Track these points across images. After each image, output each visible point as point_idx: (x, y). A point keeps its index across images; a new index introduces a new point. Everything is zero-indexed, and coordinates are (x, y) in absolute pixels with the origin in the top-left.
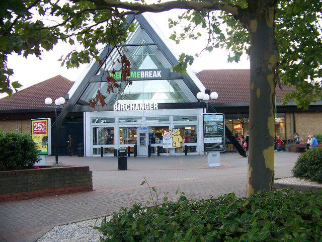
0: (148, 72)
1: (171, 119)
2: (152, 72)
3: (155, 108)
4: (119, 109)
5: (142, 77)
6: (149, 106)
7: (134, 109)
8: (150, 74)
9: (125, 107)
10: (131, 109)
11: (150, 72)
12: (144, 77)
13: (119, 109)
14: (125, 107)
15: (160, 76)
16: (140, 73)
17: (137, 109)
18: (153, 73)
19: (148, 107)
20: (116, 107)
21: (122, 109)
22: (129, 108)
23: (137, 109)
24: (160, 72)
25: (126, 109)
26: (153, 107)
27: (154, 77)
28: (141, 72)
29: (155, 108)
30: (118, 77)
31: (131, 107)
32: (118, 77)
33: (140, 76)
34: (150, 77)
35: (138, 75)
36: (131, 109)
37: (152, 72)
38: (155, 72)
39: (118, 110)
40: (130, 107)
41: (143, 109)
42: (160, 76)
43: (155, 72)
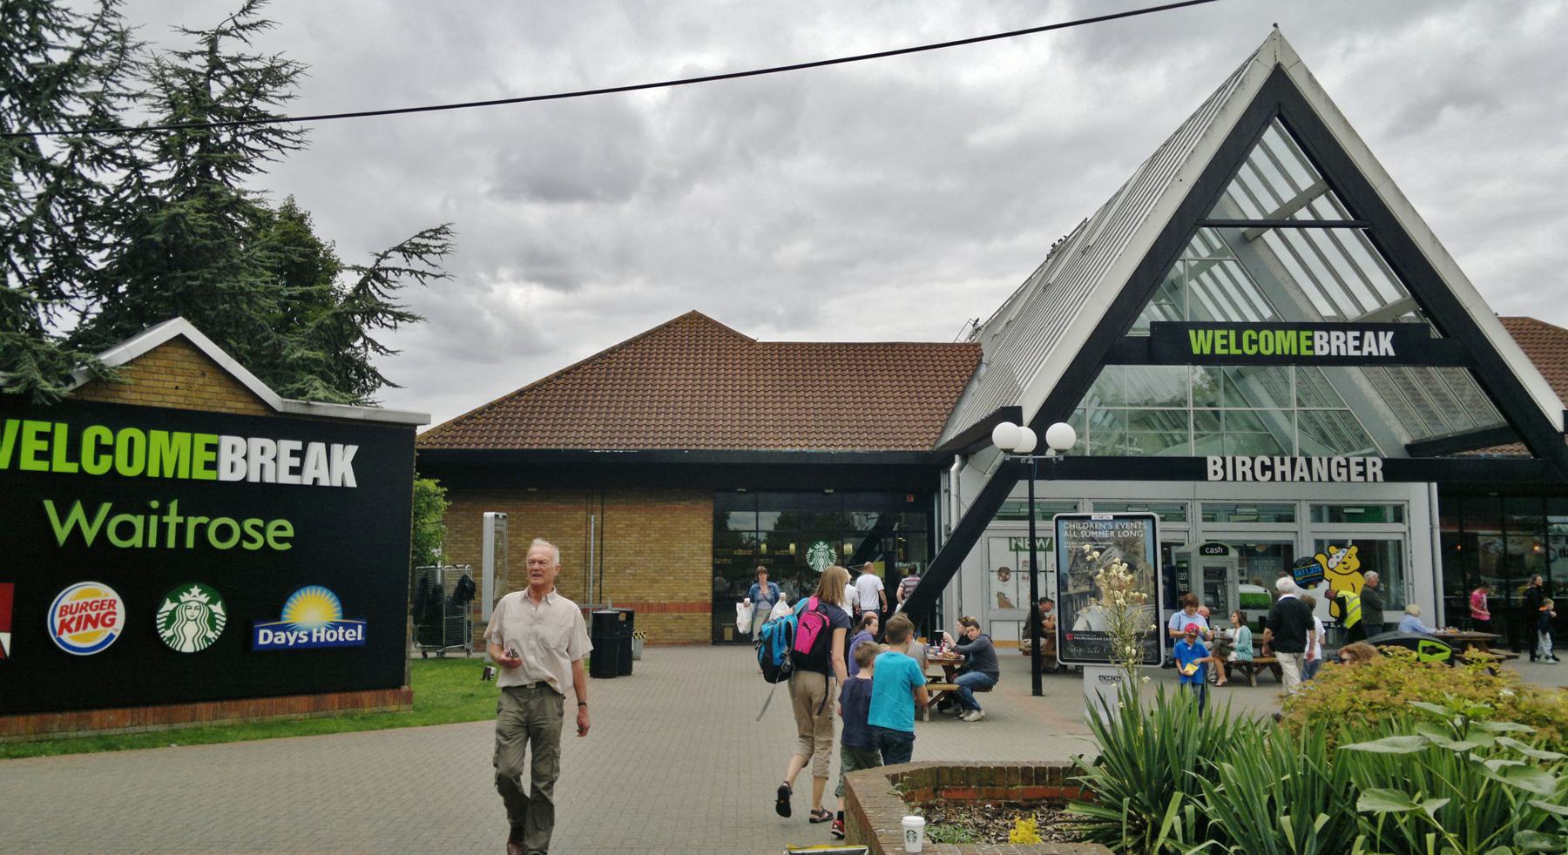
0: (1341, 334)
1: (1304, 513)
2: (1357, 334)
3: (1370, 478)
4: (1230, 477)
5: (1318, 352)
6: (1348, 466)
7: (1288, 477)
8: (1352, 343)
9: (1252, 469)
10: (1278, 477)
11: (1351, 334)
12: (1325, 352)
13: (1230, 477)
14: (1252, 469)
15: (1392, 353)
16: (1311, 338)
17: (1302, 479)
18: (1361, 339)
19: (1343, 471)
20: (1218, 468)
21: (1239, 477)
22: (1268, 474)
23: (1302, 479)
24: (1390, 334)
25: (1334, 475)
26: (1363, 474)
27: (1365, 353)
28: (1317, 334)
29: (1370, 478)
30: (1223, 347)
31: (1278, 468)
32: (1223, 347)
33: (1311, 348)
34: (1352, 353)
35: (1304, 343)
36: (1278, 477)
37: (1357, 334)
38: (1369, 335)
39: (1224, 479)
40: (1272, 468)
41: (1325, 477)
42: (1392, 353)
43: (1369, 335)
